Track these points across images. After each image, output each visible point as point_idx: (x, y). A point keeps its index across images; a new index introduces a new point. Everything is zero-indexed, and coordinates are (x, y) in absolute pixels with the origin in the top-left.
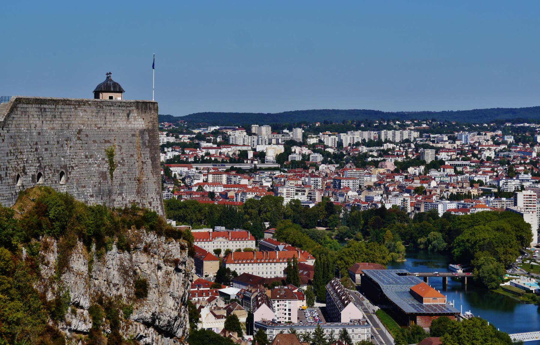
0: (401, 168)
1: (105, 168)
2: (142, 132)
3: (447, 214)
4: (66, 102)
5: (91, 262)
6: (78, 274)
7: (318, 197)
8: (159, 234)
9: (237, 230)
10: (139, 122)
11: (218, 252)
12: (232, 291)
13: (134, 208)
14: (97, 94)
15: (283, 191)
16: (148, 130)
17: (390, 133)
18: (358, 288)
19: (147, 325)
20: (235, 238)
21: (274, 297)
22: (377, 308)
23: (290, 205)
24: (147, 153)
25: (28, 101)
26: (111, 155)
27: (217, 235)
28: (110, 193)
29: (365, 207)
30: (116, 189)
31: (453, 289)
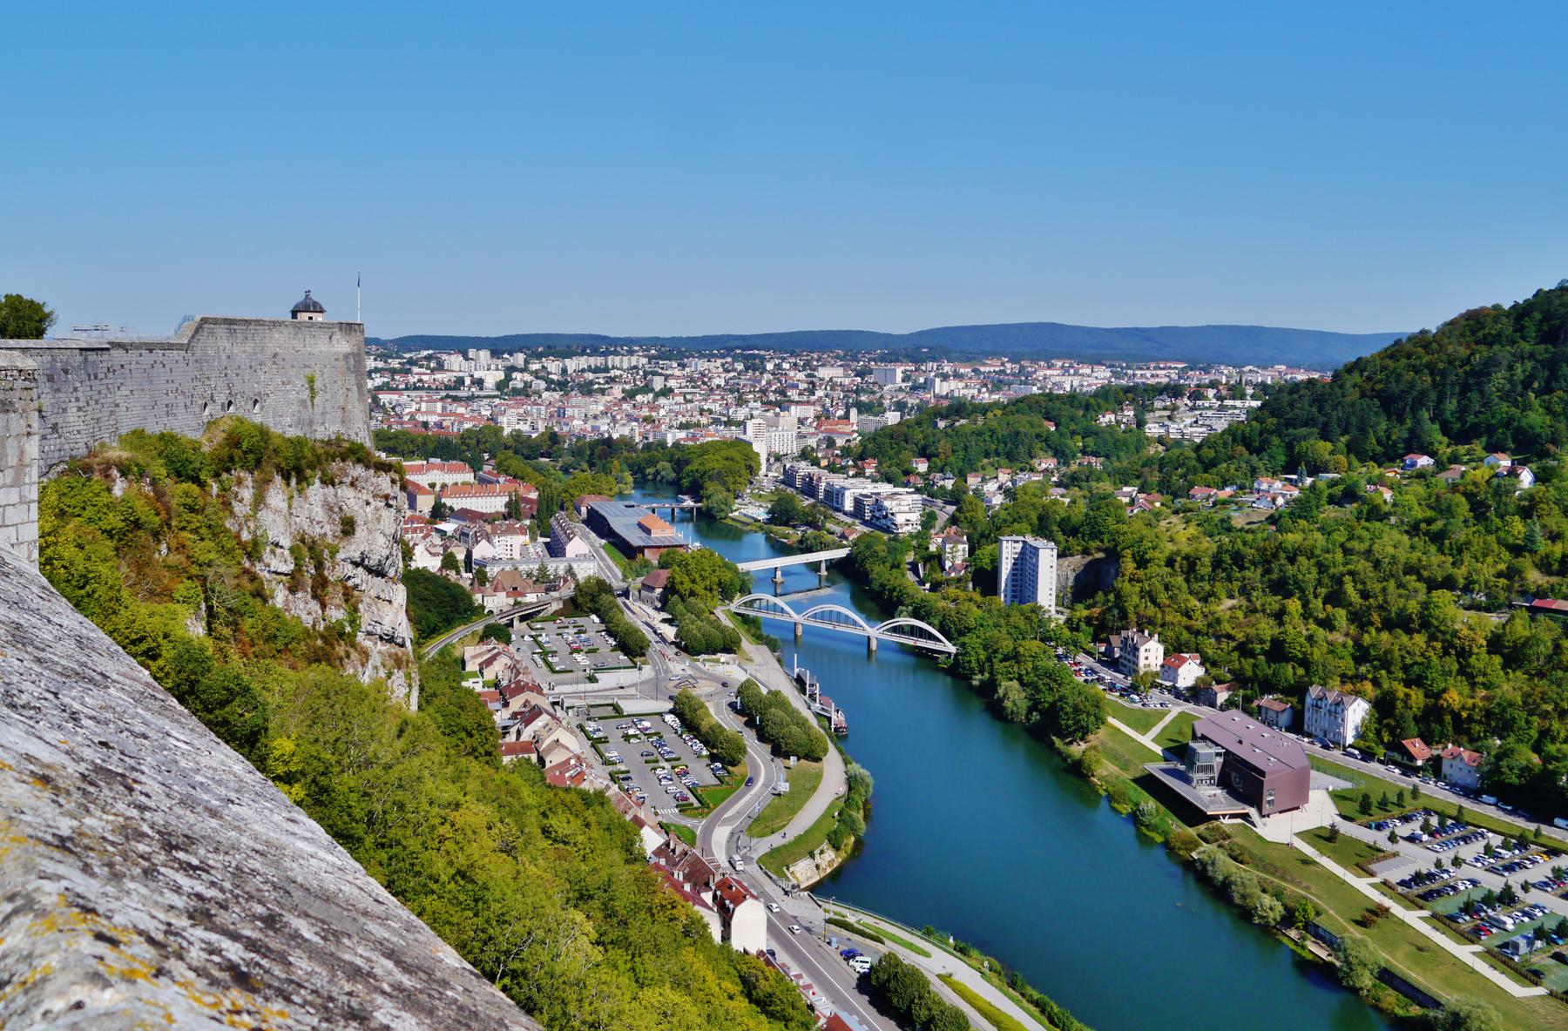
0: (630, 395)
1: (306, 395)
2: (346, 356)
3: (676, 445)
4: (258, 322)
5: (291, 498)
6: (277, 511)
7: (541, 428)
8: (367, 467)
10: (343, 345)
11: (432, 486)
12: (449, 527)
13: (338, 439)
14: (294, 314)
16: (353, 354)
17: (618, 359)
18: (584, 522)
19: (356, 564)
20: (452, 470)
21: (494, 532)
22: (604, 542)
23: (511, 435)
24: (352, 379)
25: (216, 321)
26: (311, 381)
27: (431, 467)
28: (311, 422)
29: (591, 437)
30: (318, 418)
31: (682, 521)
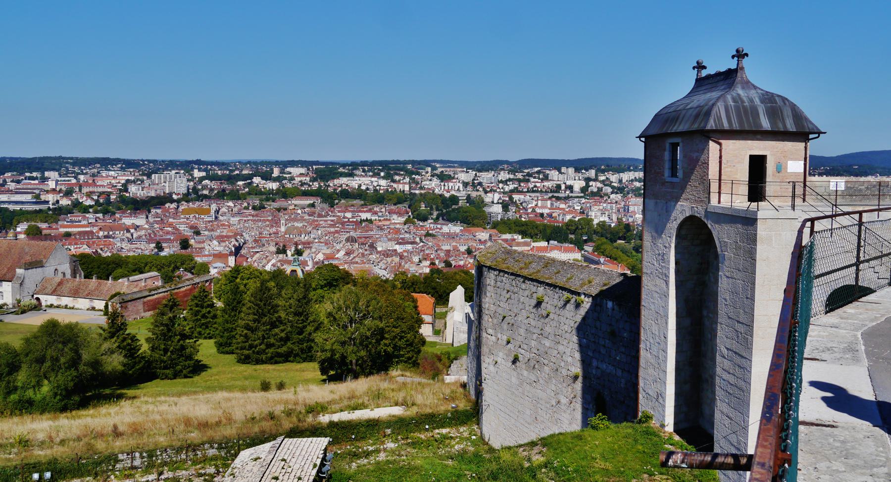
7: (615, 218)
9: (566, 245)
15: (592, 214)
20: (567, 250)
23: (598, 224)
27: (552, 249)
